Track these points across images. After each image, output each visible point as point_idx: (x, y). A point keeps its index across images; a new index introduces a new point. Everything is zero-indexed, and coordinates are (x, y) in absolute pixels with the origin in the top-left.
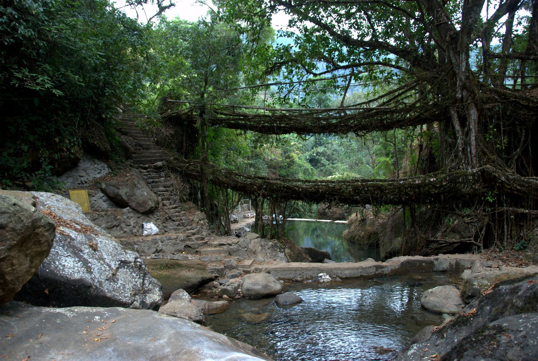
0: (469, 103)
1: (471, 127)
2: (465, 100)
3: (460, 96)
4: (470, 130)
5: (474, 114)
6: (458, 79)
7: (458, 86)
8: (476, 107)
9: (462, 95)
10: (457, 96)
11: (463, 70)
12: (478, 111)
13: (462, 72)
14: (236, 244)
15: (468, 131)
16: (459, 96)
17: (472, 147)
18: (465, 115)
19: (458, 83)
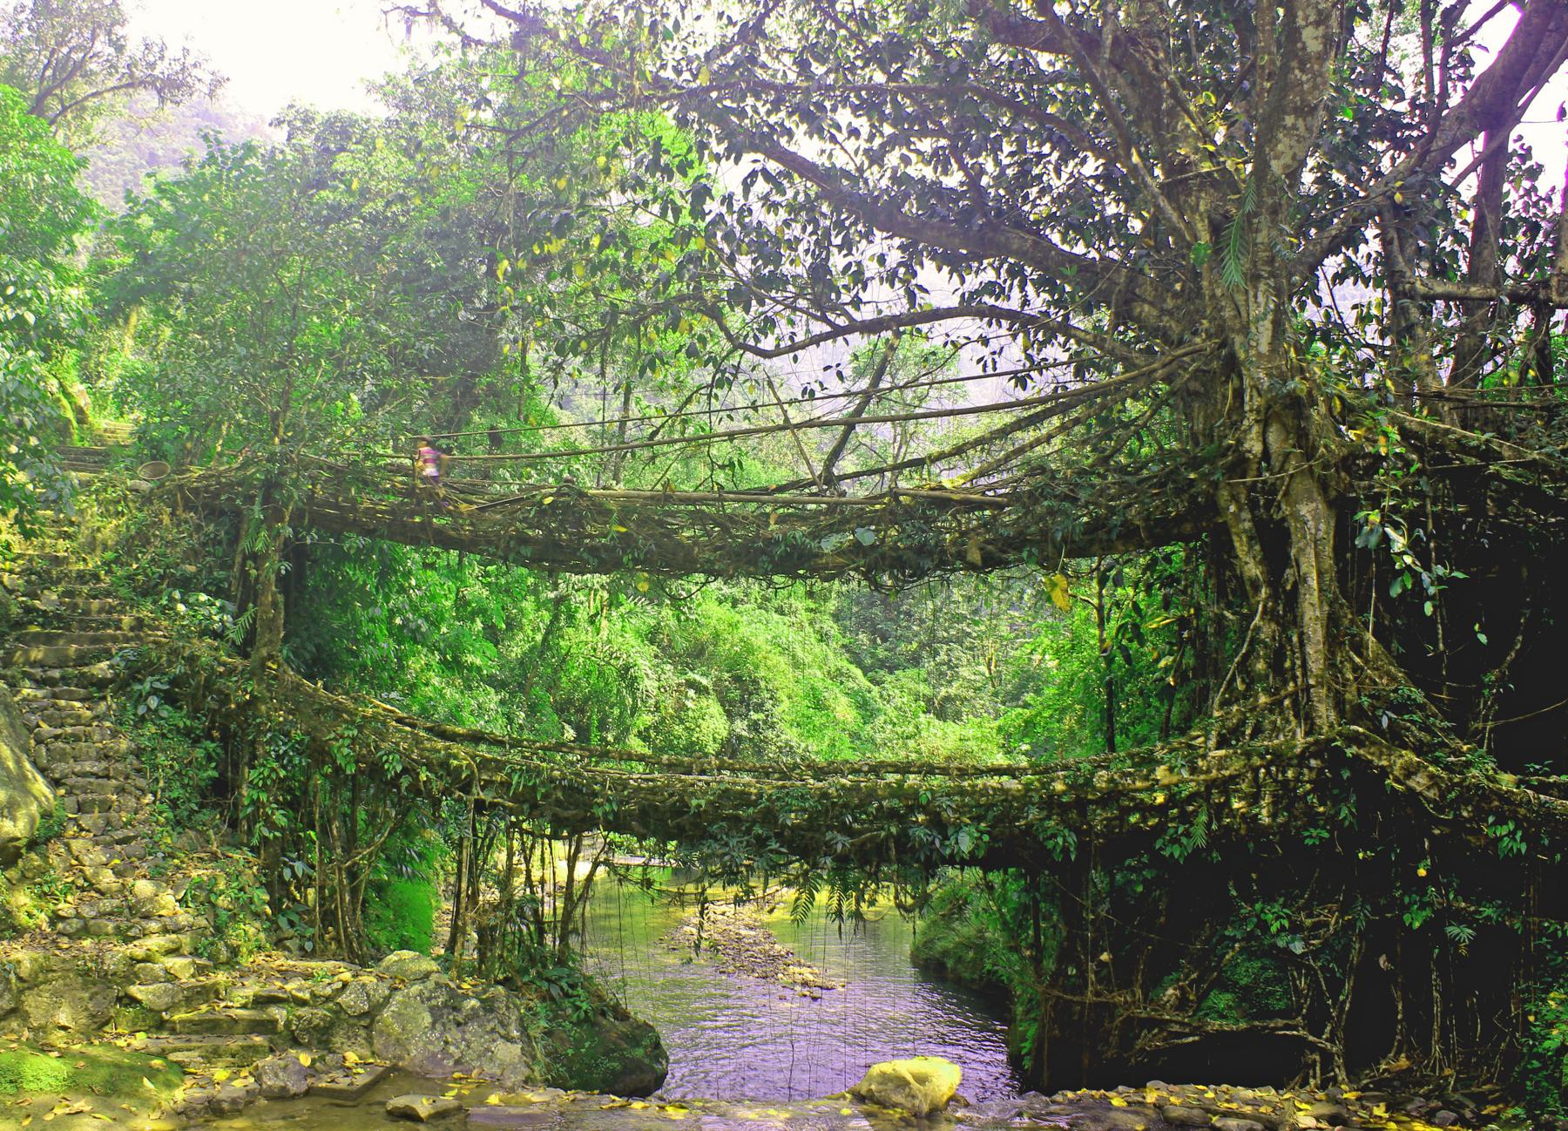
0: (1292, 476)
1: (1304, 569)
2: (1276, 464)
3: (1258, 448)
4: (1302, 580)
5: (1316, 519)
6: (1247, 382)
7: (1247, 408)
8: (1324, 486)
9: (1265, 443)
10: (1247, 446)
11: (1264, 348)
12: (1330, 504)
13: (1260, 355)
14: (328, 999)
15: (1295, 585)
16: (1254, 446)
17: (1310, 650)
18: (1284, 519)
19: (1247, 398)
